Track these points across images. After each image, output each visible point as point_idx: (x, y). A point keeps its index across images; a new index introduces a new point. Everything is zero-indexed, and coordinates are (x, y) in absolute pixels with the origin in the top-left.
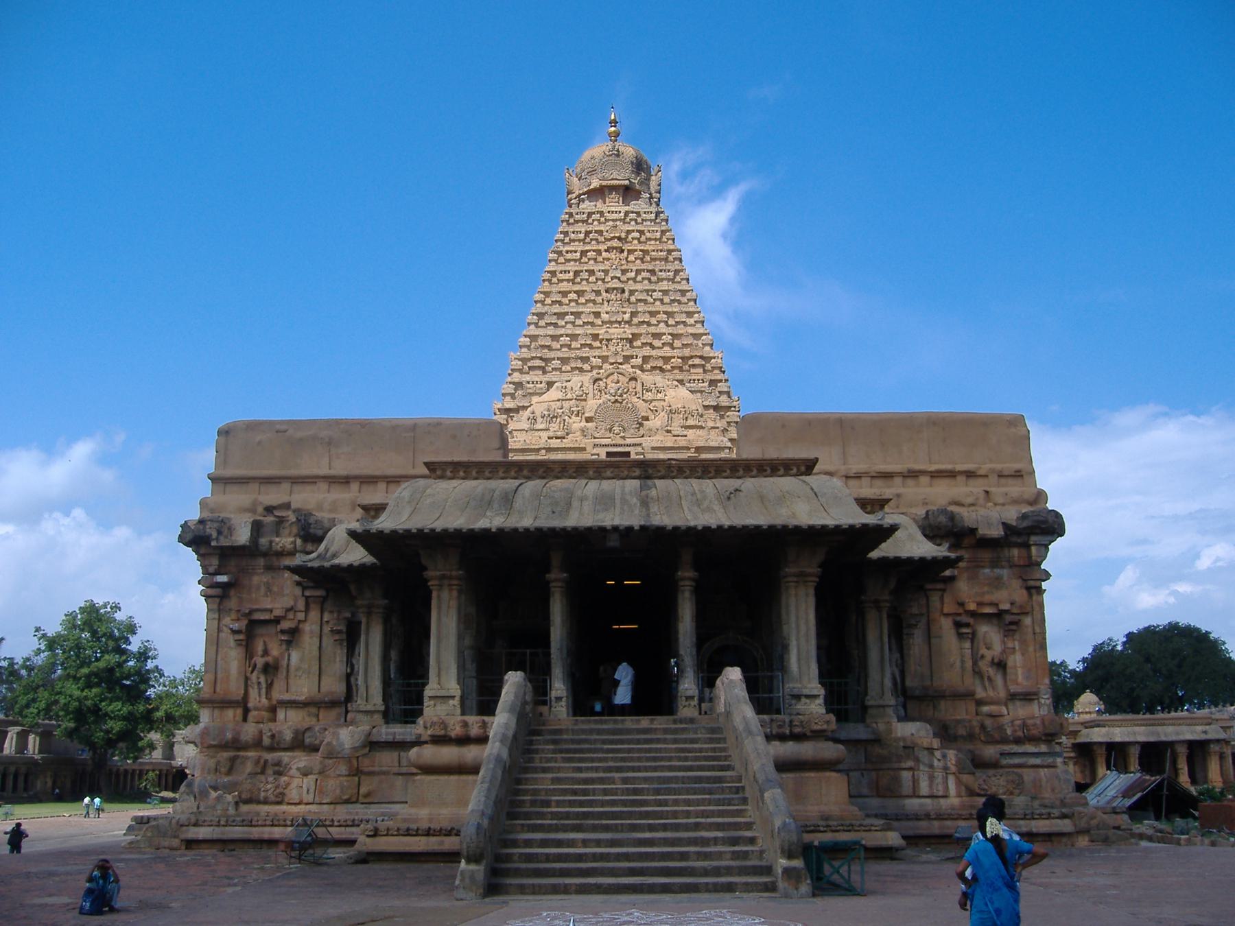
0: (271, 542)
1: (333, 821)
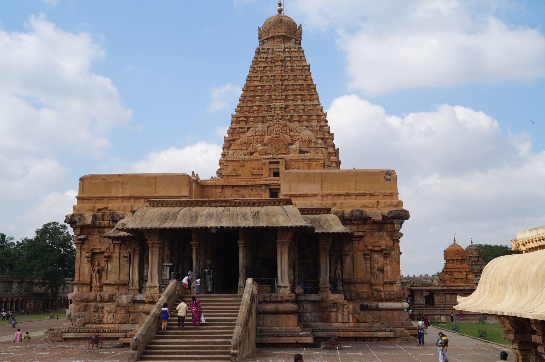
0: (100, 223)
1: (118, 330)
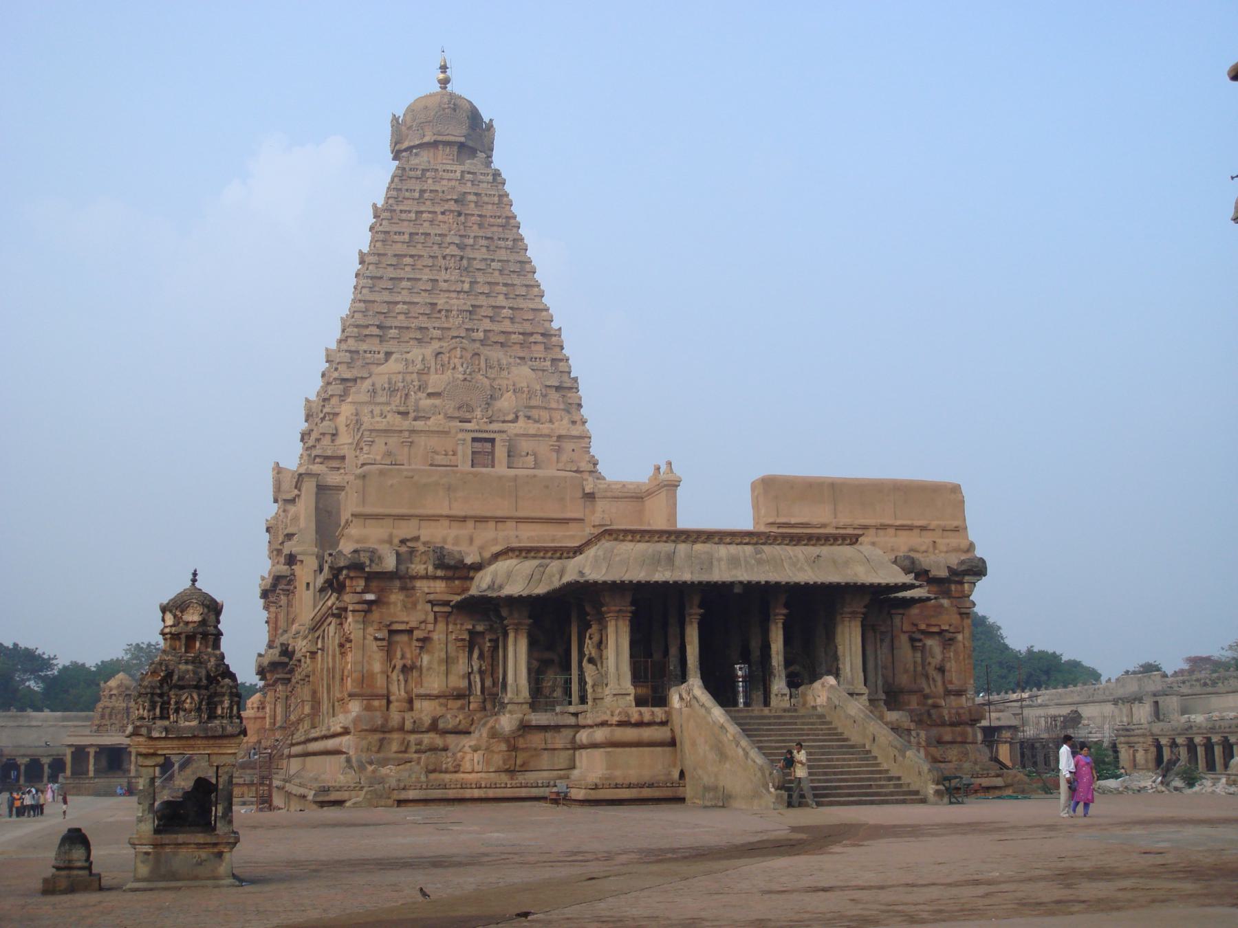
0: (408, 568)
1: (506, 784)
